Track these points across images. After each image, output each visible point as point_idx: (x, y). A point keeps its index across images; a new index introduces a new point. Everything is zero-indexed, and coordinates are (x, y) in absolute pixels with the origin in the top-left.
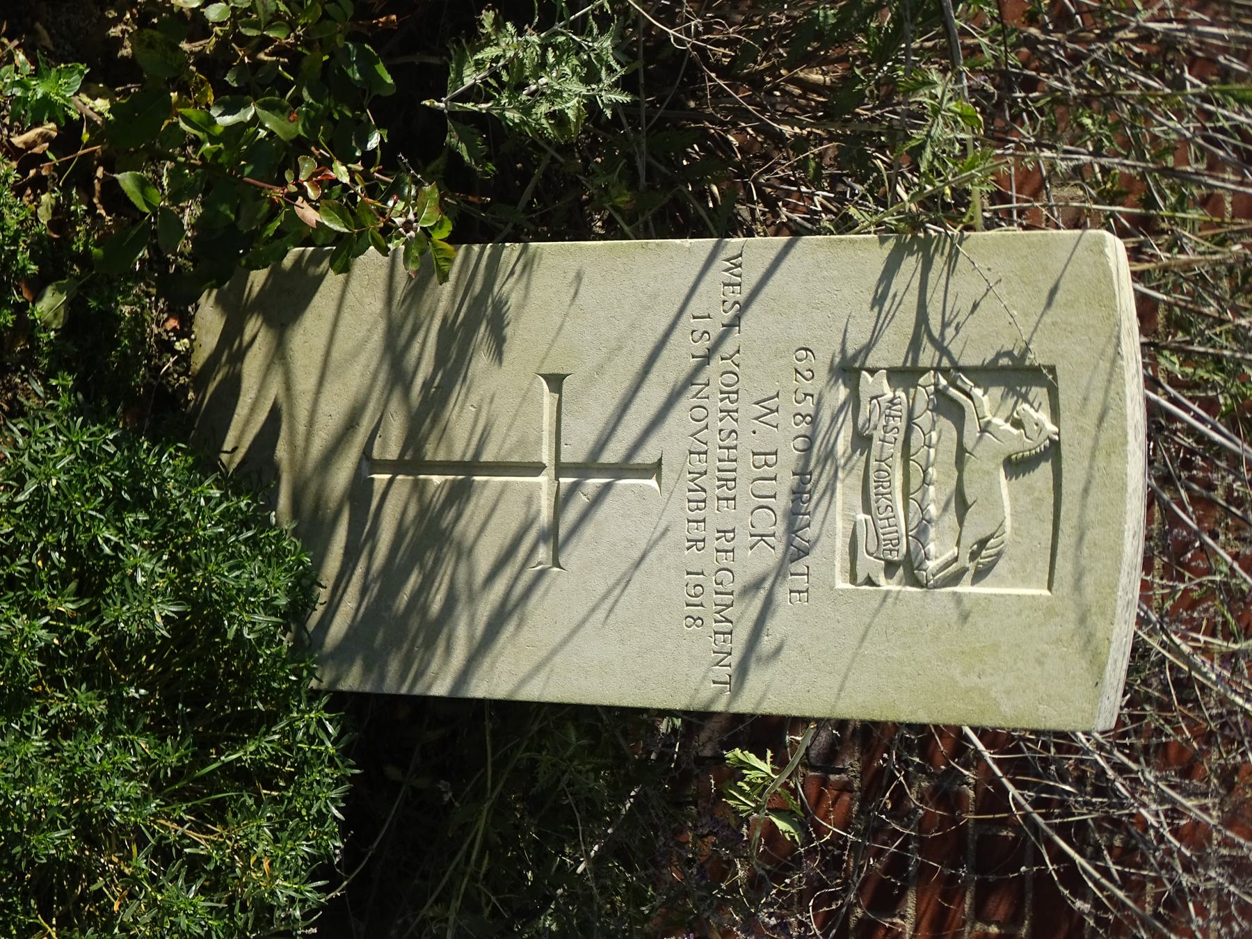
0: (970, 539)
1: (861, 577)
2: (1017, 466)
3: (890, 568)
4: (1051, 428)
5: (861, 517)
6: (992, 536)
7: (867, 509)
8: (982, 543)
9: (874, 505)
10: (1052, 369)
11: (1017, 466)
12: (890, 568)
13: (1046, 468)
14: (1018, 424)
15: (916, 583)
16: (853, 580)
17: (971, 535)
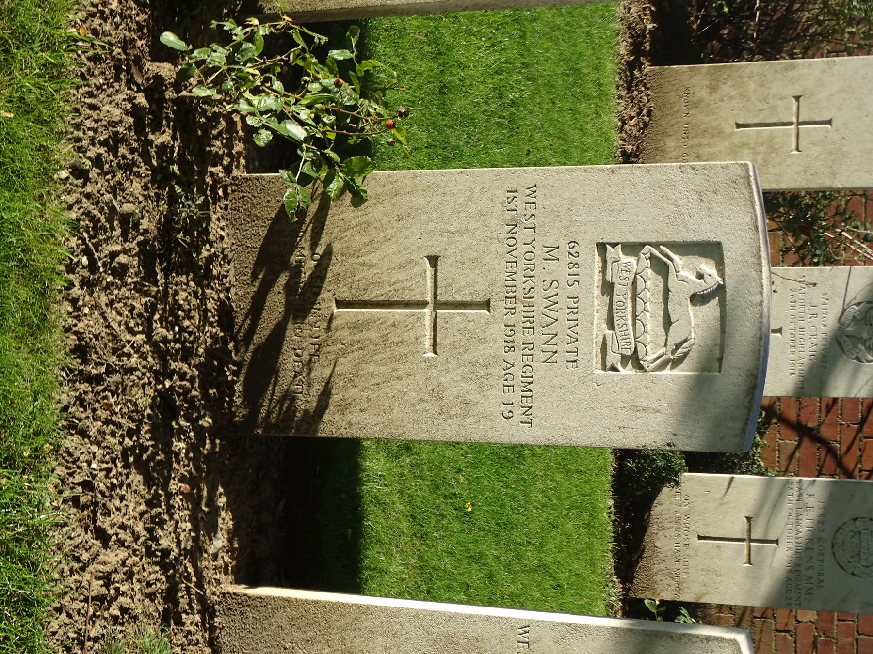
0: (672, 342)
1: (608, 365)
2: (698, 299)
3: (625, 360)
4: (720, 280)
5: (611, 332)
6: (686, 340)
7: (611, 325)
8: (678, 346)
9: (616, 323)
10: (719, 245)
11: (698, 299)
12: (625, 360)
13: (715, 302)
14: (700, 276)
15: (641, 368)
16: (604, 368)
17: (673, 340)
